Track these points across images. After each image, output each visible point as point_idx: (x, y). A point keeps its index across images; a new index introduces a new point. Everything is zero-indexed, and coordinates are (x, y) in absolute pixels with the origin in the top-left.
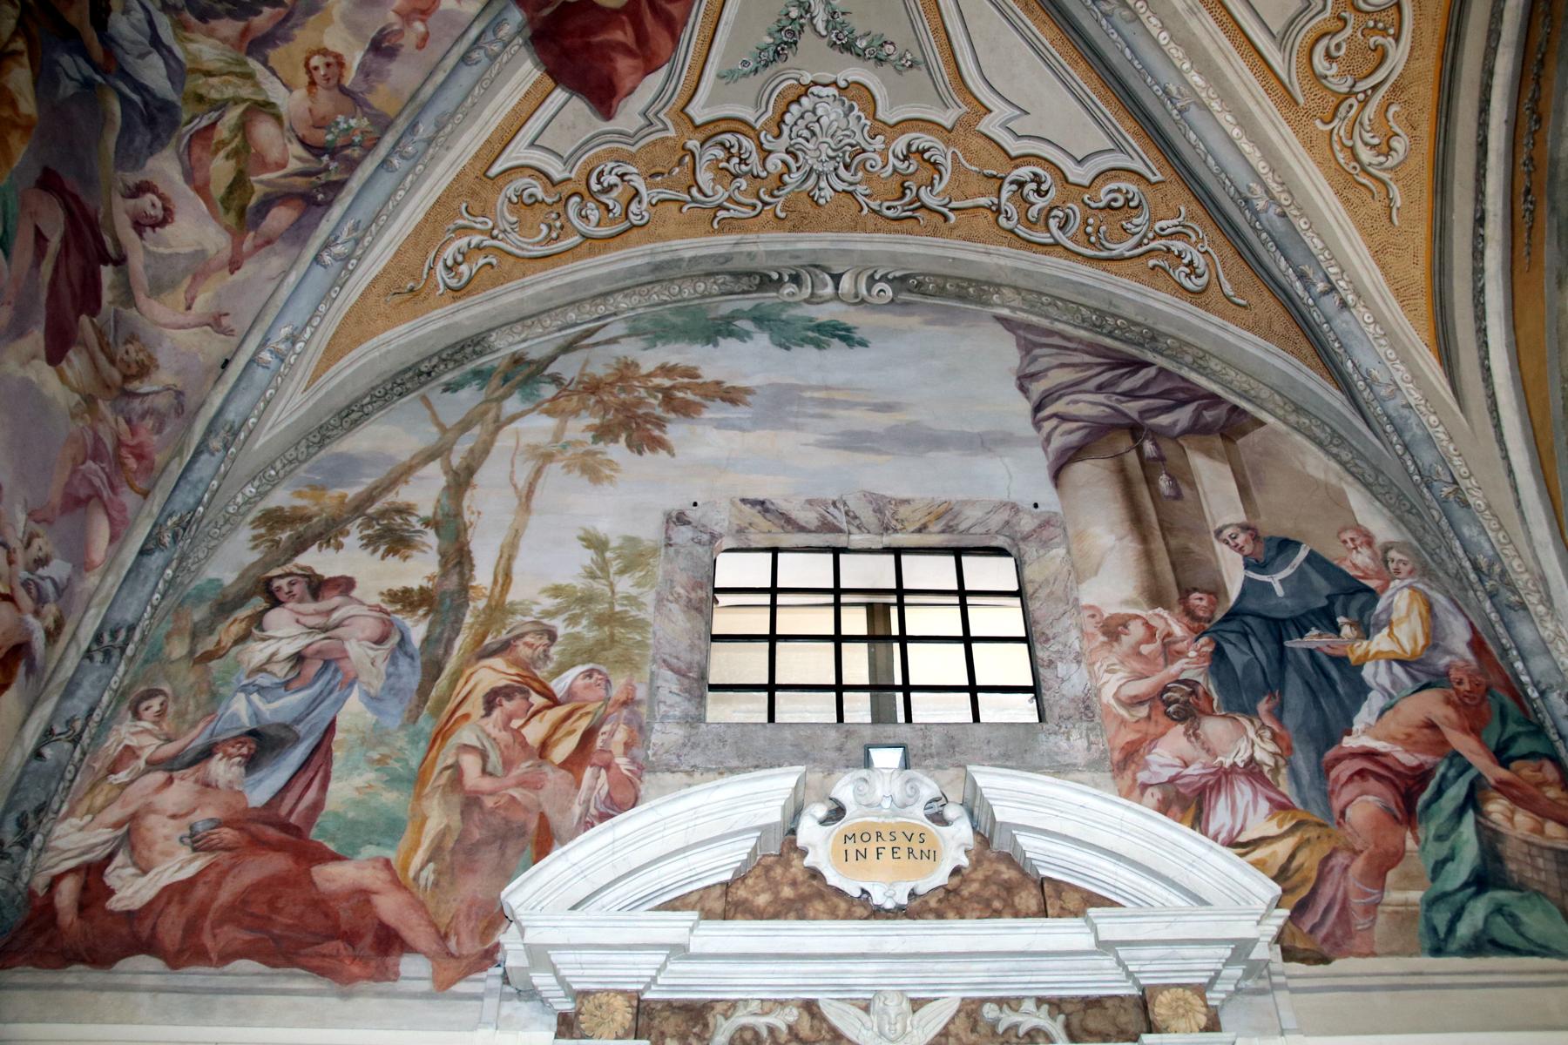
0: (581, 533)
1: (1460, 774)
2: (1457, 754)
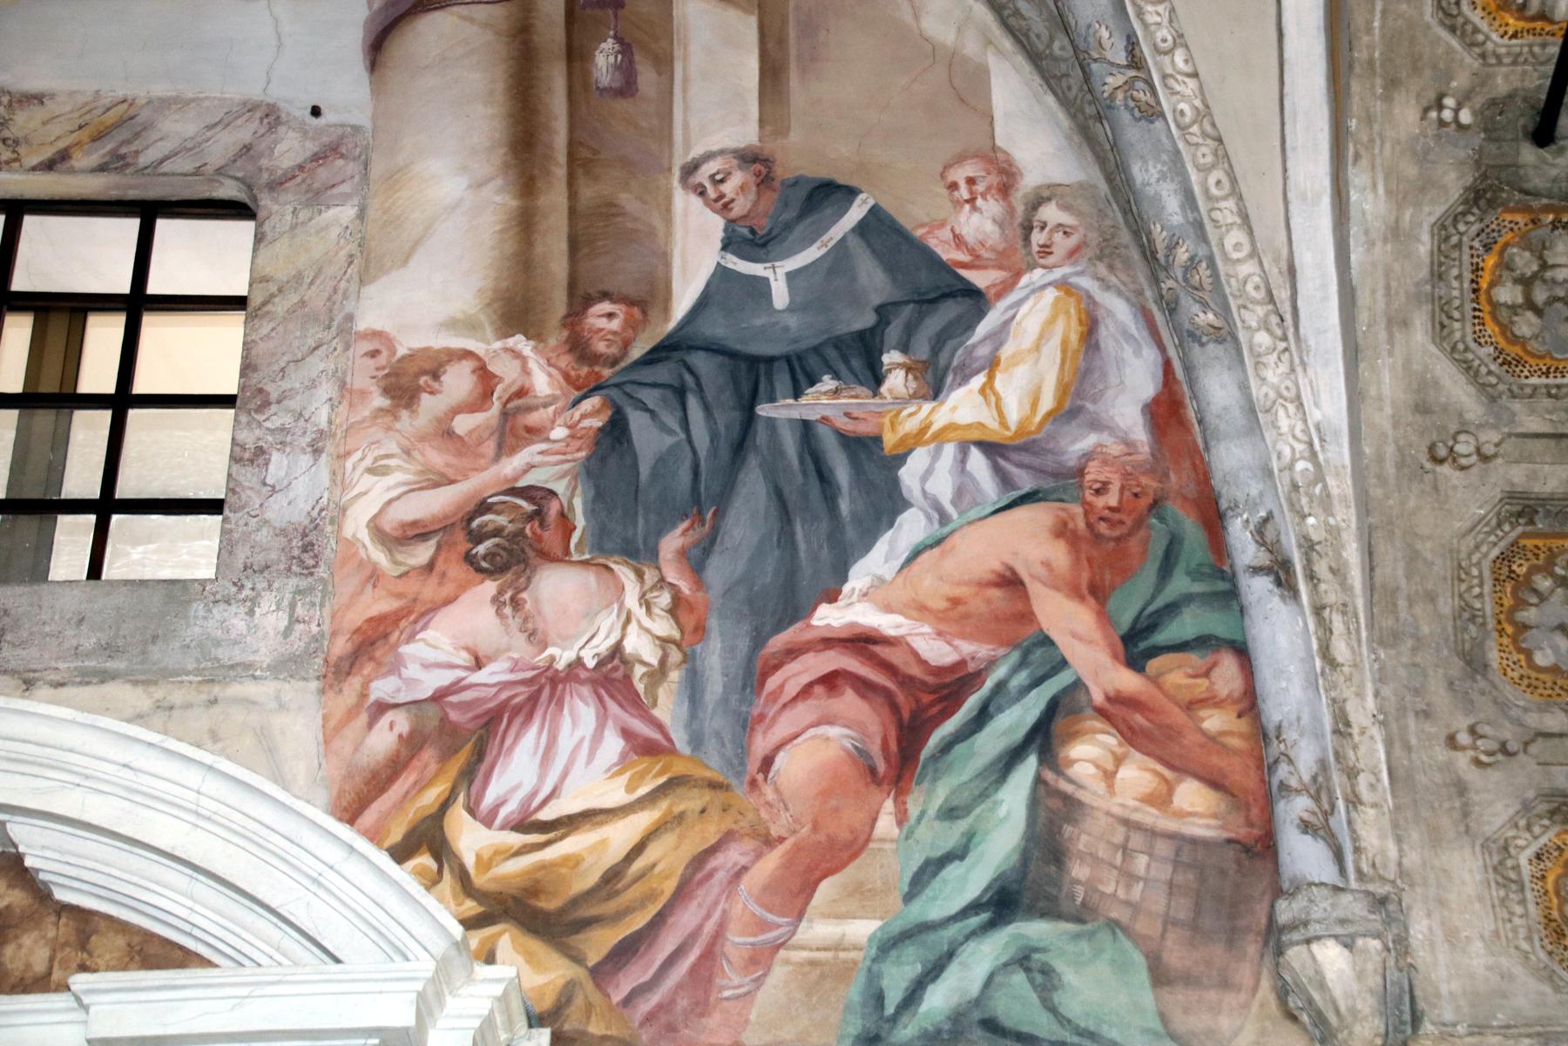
1: (1037, 682)
2: (1047, 641)
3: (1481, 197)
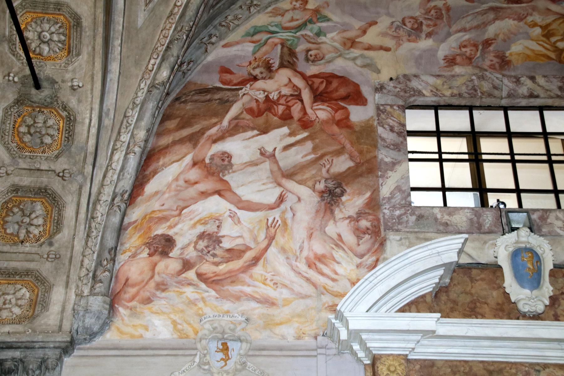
3: (19, 102)
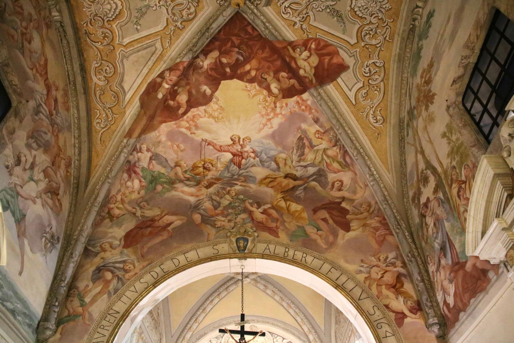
0: (441, 137)
